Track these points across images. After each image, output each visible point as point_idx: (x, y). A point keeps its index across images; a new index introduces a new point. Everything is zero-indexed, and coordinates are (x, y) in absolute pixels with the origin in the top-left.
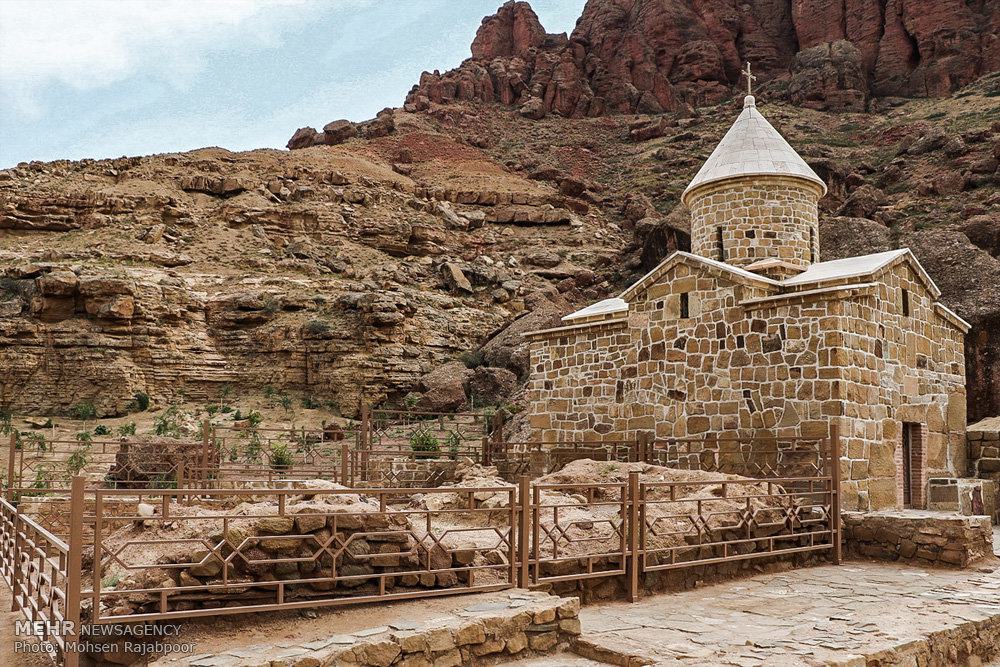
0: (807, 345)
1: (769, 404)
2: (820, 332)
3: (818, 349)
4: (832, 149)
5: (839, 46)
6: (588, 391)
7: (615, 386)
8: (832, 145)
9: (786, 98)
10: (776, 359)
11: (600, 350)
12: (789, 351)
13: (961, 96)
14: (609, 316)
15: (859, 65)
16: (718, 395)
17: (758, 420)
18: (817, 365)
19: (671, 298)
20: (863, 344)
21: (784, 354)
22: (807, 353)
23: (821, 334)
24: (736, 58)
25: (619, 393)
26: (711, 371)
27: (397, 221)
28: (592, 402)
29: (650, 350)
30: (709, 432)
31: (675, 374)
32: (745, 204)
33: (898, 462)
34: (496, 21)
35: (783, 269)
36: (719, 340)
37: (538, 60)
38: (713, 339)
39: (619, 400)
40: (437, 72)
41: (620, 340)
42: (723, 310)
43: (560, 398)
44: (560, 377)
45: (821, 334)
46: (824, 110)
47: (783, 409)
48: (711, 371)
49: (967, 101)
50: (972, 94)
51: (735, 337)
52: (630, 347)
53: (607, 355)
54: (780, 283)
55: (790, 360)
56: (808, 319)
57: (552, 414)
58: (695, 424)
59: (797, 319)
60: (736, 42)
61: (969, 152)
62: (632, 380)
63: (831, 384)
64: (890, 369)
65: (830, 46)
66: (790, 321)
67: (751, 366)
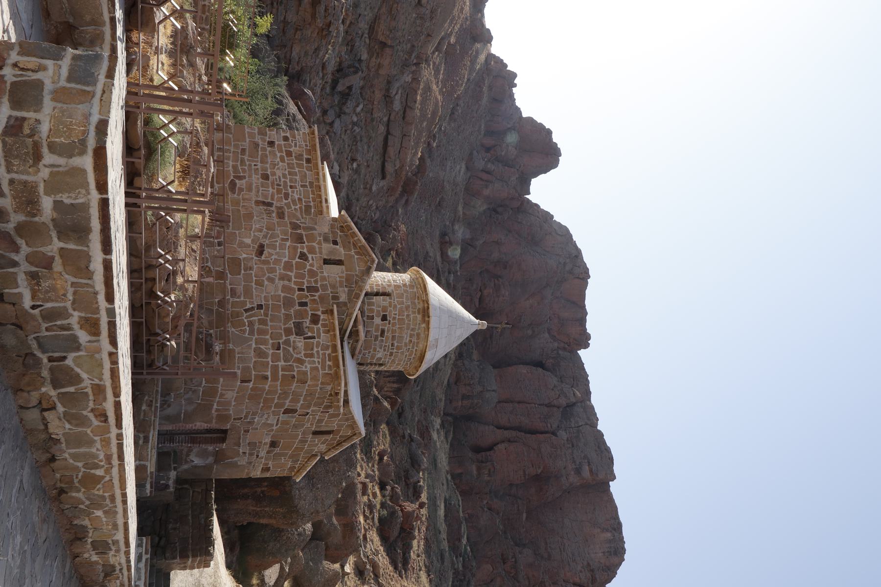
0: (298, 356)
1: (251, 324)
2: (309, 366)
3: (295, 364)
4: (419, 388)
6: (266, 177)
7: (269, 200)
10: (288, 332)
11: (300, 190)
12: (294, 342)
13: (447, 480)
14: (326, 201)
16: (259, 283)
17: (238, 315)
18: (281, 363)
19: (341, 252)
20: (295, 400)
21: (292, 338)
22: (292, 356)
23: (307, 367)
25: (264, 203)
26: (280, 279)
27: (400, 34)
28: (256, 179)
30: (228, 274)
31: (278, 250)
32: (408, 316)
33: (195, 425)
35: (357, 341)
36: (305, 287)
38: (306, 283)
39: (258, 203)
40: (515, 85)
41: (308, 208)
42: (329, 292)
43: (260, 153)
44: (279, 155)
45: (307, 367)
48: (280, 279)
49: (443, 485)
50: (448, 488)
51: (307, 300)
52: (302, 215)
53: (296, 197)
54: (346, 338)
56: (319, 358)
57: (246, 144)
58: (235, 264)
61: (407, 485)
62: (274, 215)
63: (266, 373)
64: (272, 420)
65: (493, 391)
66: (318, 344)
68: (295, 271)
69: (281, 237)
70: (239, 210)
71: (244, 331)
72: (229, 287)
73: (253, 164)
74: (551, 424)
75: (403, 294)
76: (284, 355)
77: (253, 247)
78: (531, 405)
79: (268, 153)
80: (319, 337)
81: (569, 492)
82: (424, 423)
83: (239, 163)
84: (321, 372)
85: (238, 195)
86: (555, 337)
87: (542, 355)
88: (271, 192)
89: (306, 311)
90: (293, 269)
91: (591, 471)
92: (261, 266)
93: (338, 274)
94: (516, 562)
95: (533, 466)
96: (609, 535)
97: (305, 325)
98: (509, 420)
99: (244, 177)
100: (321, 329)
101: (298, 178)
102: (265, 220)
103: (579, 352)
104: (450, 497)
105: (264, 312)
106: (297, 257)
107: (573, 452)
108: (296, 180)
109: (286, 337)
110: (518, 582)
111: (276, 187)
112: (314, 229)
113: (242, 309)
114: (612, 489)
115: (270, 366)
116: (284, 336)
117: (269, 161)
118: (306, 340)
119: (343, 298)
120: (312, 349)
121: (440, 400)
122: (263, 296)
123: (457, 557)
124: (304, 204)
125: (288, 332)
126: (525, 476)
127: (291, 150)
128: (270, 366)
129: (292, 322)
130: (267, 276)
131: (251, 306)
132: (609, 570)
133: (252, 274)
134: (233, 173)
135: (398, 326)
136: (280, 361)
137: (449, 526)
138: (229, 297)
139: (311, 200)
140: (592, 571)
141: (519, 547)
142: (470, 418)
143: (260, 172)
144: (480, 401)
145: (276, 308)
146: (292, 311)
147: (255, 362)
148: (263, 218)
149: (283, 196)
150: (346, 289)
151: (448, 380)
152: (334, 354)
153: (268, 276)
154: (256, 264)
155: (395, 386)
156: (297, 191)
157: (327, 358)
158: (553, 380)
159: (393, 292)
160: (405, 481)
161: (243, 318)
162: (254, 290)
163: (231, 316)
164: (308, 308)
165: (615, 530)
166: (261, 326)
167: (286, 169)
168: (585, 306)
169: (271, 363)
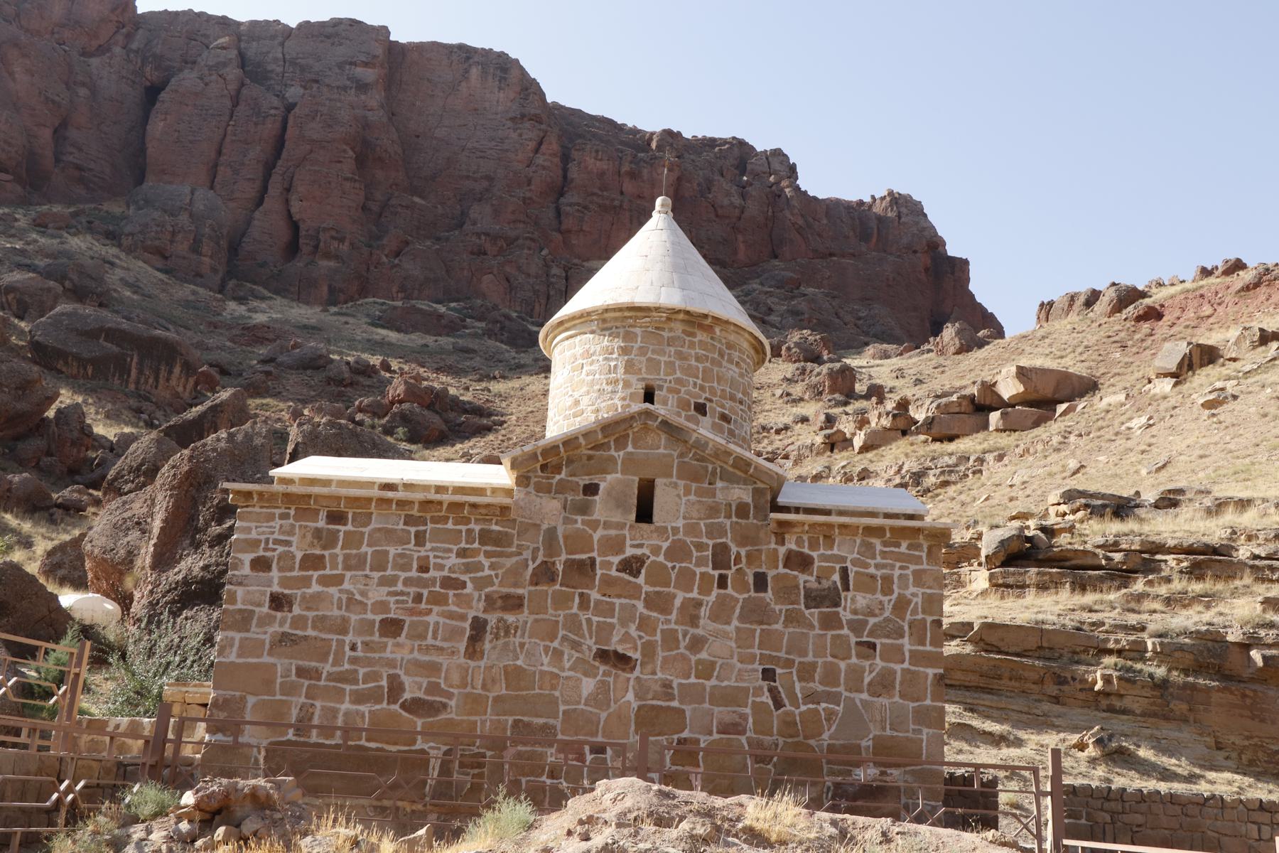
1: (811, 697)
2: (912, 589)
3: (908, 617)
4: (171, 327)
5: (203, 200)
7: (467, 625)
8: (170, 321)
9: (112, 237)
10: (830, 622)
11: (433, 549)
12: (855, 612)
15: (225, 231)
16: (706, 670)
17: (789, 725)
18: (906, 643)
21: (845, 615)
22: (887, 620)
23: (915, 593)
28: (400, 650)
29: (560, 568)
31: (614, 621)
32: (698, 359)
36: (716, 573)
38: (703, 569)
39: (473, 650)
41: (486, 537)
42: (728, 522)
43: (310, 632)
44: (315, 588)
46: (166, 272)
47: (840, 709)
49: (346, 323)
50: (354, 316)
53: (453, 560)
55: (857, 627)
56: (893, 567)
57: (283, 666)
58: (649, 719)
59: (872, 562)
60: (55, 131)
61: (351, 384)
62: (510, 618)
63: (930, 677)
65: (192, 193)
67: (779, 626)
68: (672, 590)
69: (575, 610)
70: (497, 699)
71: (830, 715)
72: (716, 736)
73: (348, 653)
74: (272, 108)
75: (650, 360)
76: (888, 637)
77: (604, 674)
78: (229, 132)
79: (311, 614)
80: (844, 559)
81: (393, 114)
82: (235, 332)
83: (348, 687)
84: (925, 566)
85: (450, 696)
86: (100, 46)
88: (442, 620)
89: (777, 578)
90: (668, 594)
91: (366, 64)
92: (659, 663)
93: (678, 496)
94: (487, 234)
95: (340, 162)
96: (475, 72)
97: (815, 585)
98: (249, 179)
99: (393, 679)
100: (822, 551)
101: (393, 551)
102: (526, 640)
103: (139, 12)
104: (368, 315)
105: (782, 668)
106: (631, 579)
107: (328, 86)
108: (401, 555)
109: (842, 627)
110: (517, 239)
111: (423, 606)
112: (551, 532)
113: (775, 713)
114: (403, 40)
115: (913, 668)
116: (842, 632)
117: (336, 612)
118: (851, 587)
119: (742, 494)
120: (873, 577)
121: (194, 293)
122: (739, 665)
123: (465, 327)
124: (476, 545)
125: (830, 622)
126: (355, 181)
127: (299, 555)
128: (913, 668)
129: (807, 612)
130: (687, 653)
131: (767, 694)
132: (527, 89)
133: (680, 684)
134: (379, 701)
135: (715, 385)
136: (903, 645)
137: (415, 328)
138: (743, 739)
139: (463, 528)
140: (523, 116)
141: (464, 223)
142: (234, 249)
143: (376, 637)
144: (210, 222)
145: (768, 640)
146: (777, 608)
147: (902, 696)
148: (522, 645)
149: (451, 593)
150: (719, 484)
151: (158, 270)
152: (888, 535)
153: (686, 648)
154: (654, 673)
155: (177, 370)
156: (435, 557)
157: (892, 549)
158: (187, 79)
159: (643, 379)
160: (345, 386)
161: (797, 712)
162: (725, 683)
163: (791, 736)
164: (771, 574)
165: (468, 58)
166: (817, 677)
167: (366, 576)
169: (906, 665)
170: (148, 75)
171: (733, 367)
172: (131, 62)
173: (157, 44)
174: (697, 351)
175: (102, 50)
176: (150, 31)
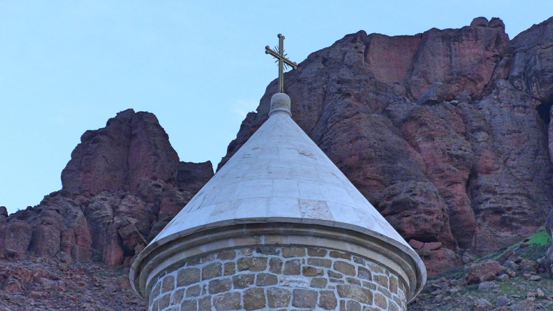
24: (468, 208)
32: (238, 283)
34: (104, 138)
37: (165, 200)
60: (468, 184)
86: (486, 86)
87: (525, 107)
103: (511, 37)
168: (420, 36)
170: (535, 94)
171: (301, 278)
172: (517, 88)
173: (535, 62)
174: (237, 273)
175: (490, 88)
176: (525, 51)
